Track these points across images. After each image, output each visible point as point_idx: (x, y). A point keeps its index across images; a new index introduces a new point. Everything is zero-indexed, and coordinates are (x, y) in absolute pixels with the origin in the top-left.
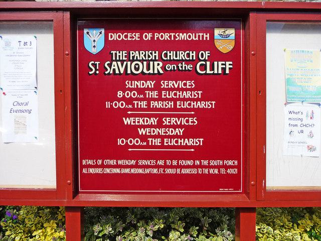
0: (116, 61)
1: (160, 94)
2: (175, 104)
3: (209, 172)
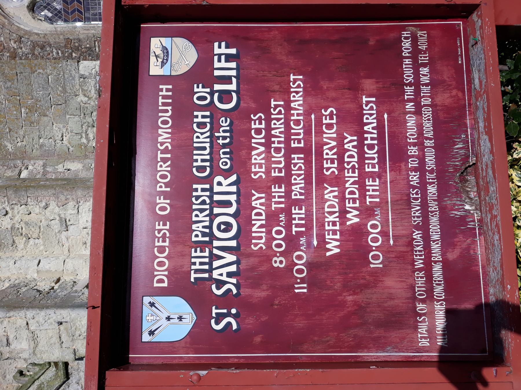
0: (210, 271)
1: (278, 181)
2: (297, 151)
3: (427, 85)
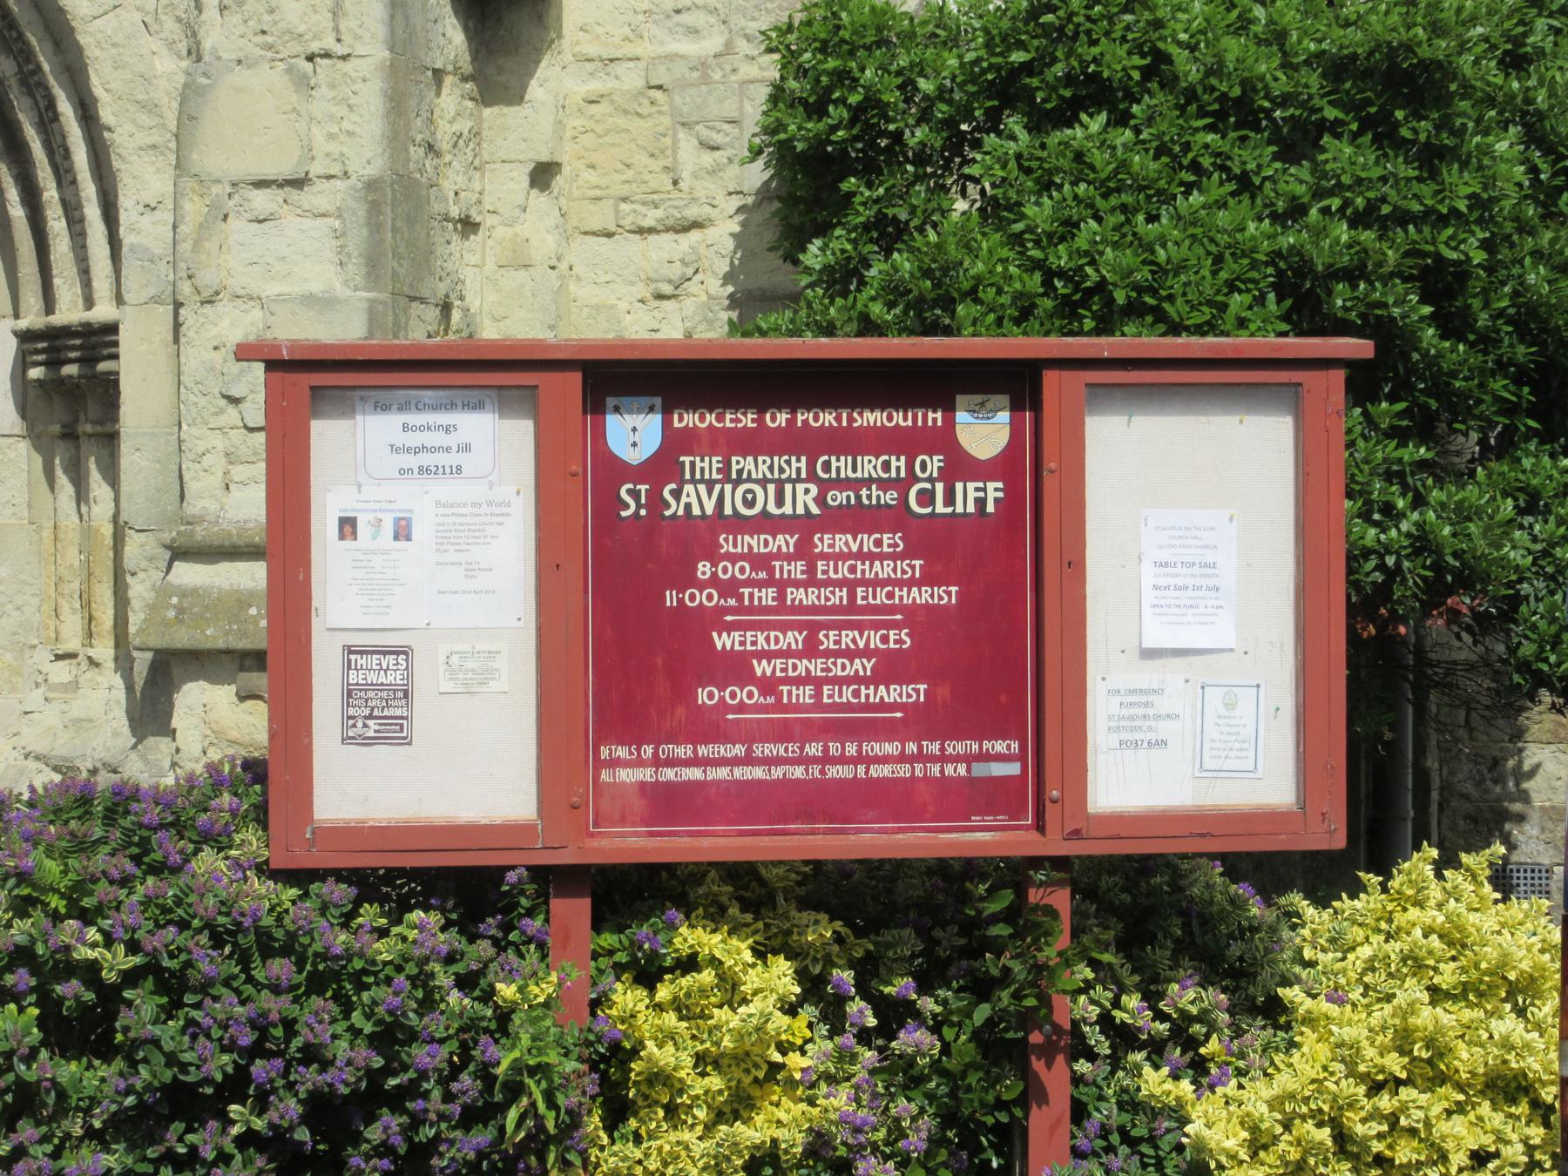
0: (693, 481)
1: (811, 569)
2: (852, 596)
3: (942, 772)
